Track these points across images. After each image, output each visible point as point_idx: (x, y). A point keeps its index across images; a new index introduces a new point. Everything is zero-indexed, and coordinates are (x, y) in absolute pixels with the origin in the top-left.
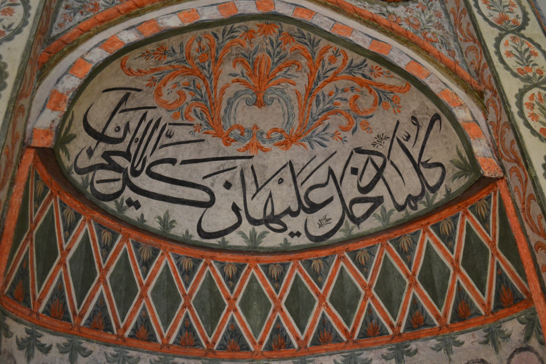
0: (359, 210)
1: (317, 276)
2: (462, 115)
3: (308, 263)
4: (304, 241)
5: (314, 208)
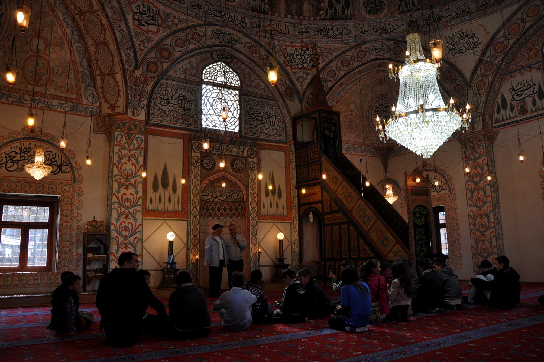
0: (229, 198)
1: (222, 206)
2: (244, 193)
3: (220, 204)
4: (220, 201)
5: (222, 196)
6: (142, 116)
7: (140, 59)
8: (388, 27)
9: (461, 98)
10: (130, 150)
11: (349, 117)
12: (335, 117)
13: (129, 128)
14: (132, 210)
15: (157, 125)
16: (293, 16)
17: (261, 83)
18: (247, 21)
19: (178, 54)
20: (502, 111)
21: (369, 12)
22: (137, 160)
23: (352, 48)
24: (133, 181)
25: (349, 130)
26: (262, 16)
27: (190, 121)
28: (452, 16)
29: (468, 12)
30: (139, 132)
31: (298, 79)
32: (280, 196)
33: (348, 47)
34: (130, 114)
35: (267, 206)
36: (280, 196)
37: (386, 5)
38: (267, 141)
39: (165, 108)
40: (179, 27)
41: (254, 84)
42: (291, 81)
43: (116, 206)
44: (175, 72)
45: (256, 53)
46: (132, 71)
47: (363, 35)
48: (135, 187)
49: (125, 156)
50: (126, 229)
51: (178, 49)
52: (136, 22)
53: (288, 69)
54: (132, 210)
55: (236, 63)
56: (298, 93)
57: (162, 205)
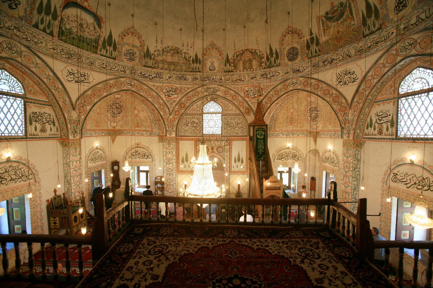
6: (174, 135)
7: (171, 111)
8: (301, 69)
9: (344, 116)
10: (170, 150)
11: (291, 116)
12: (264, 127)
13: (169, 141)
14: (171, 173)
15: (183, 136)
16: (247, 70)
17: (234, 108)
18: (223, 78)
19: (188, 104)
20: (369, 128)
21: (290, 60)
22: (172, 153)
23: (280, 84)
24: (171, 161)
25: (290, 124)
26: (230, 73)
27: (197, 132)
28: (340, 59)
29: (350, 56)
30: (173, 142)
31: (252, 103)
32: (242, 162)
33: (278, 83)
34: (168, 136)
35: (235, 167)
36: (242, 162)
37: (300, 55)
38: (236, 136)
39: (186, 128)
40: (188, 91)
41: (229, 109)
42: (248, 105)
43: (166, 171)
44: (190, 111)
45: (228, 94)
46: (168, 117)
47: (287, 75)
48: (172, 164)
49: (168, 152)
50: (170, 179)
51: (188, 102)
52: (167, 96)
53: (247, 99)
54: (171, 173)
55: (220, 100)
56: (253, 110)
57: (186, 168)
